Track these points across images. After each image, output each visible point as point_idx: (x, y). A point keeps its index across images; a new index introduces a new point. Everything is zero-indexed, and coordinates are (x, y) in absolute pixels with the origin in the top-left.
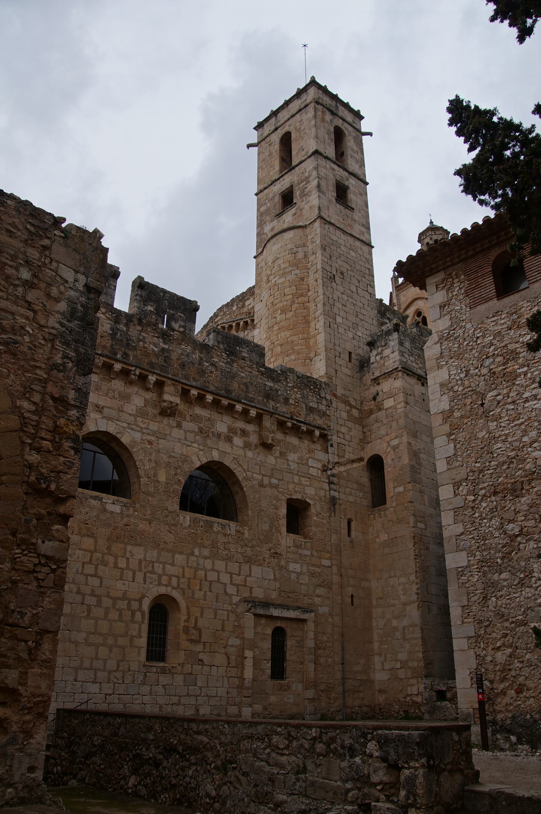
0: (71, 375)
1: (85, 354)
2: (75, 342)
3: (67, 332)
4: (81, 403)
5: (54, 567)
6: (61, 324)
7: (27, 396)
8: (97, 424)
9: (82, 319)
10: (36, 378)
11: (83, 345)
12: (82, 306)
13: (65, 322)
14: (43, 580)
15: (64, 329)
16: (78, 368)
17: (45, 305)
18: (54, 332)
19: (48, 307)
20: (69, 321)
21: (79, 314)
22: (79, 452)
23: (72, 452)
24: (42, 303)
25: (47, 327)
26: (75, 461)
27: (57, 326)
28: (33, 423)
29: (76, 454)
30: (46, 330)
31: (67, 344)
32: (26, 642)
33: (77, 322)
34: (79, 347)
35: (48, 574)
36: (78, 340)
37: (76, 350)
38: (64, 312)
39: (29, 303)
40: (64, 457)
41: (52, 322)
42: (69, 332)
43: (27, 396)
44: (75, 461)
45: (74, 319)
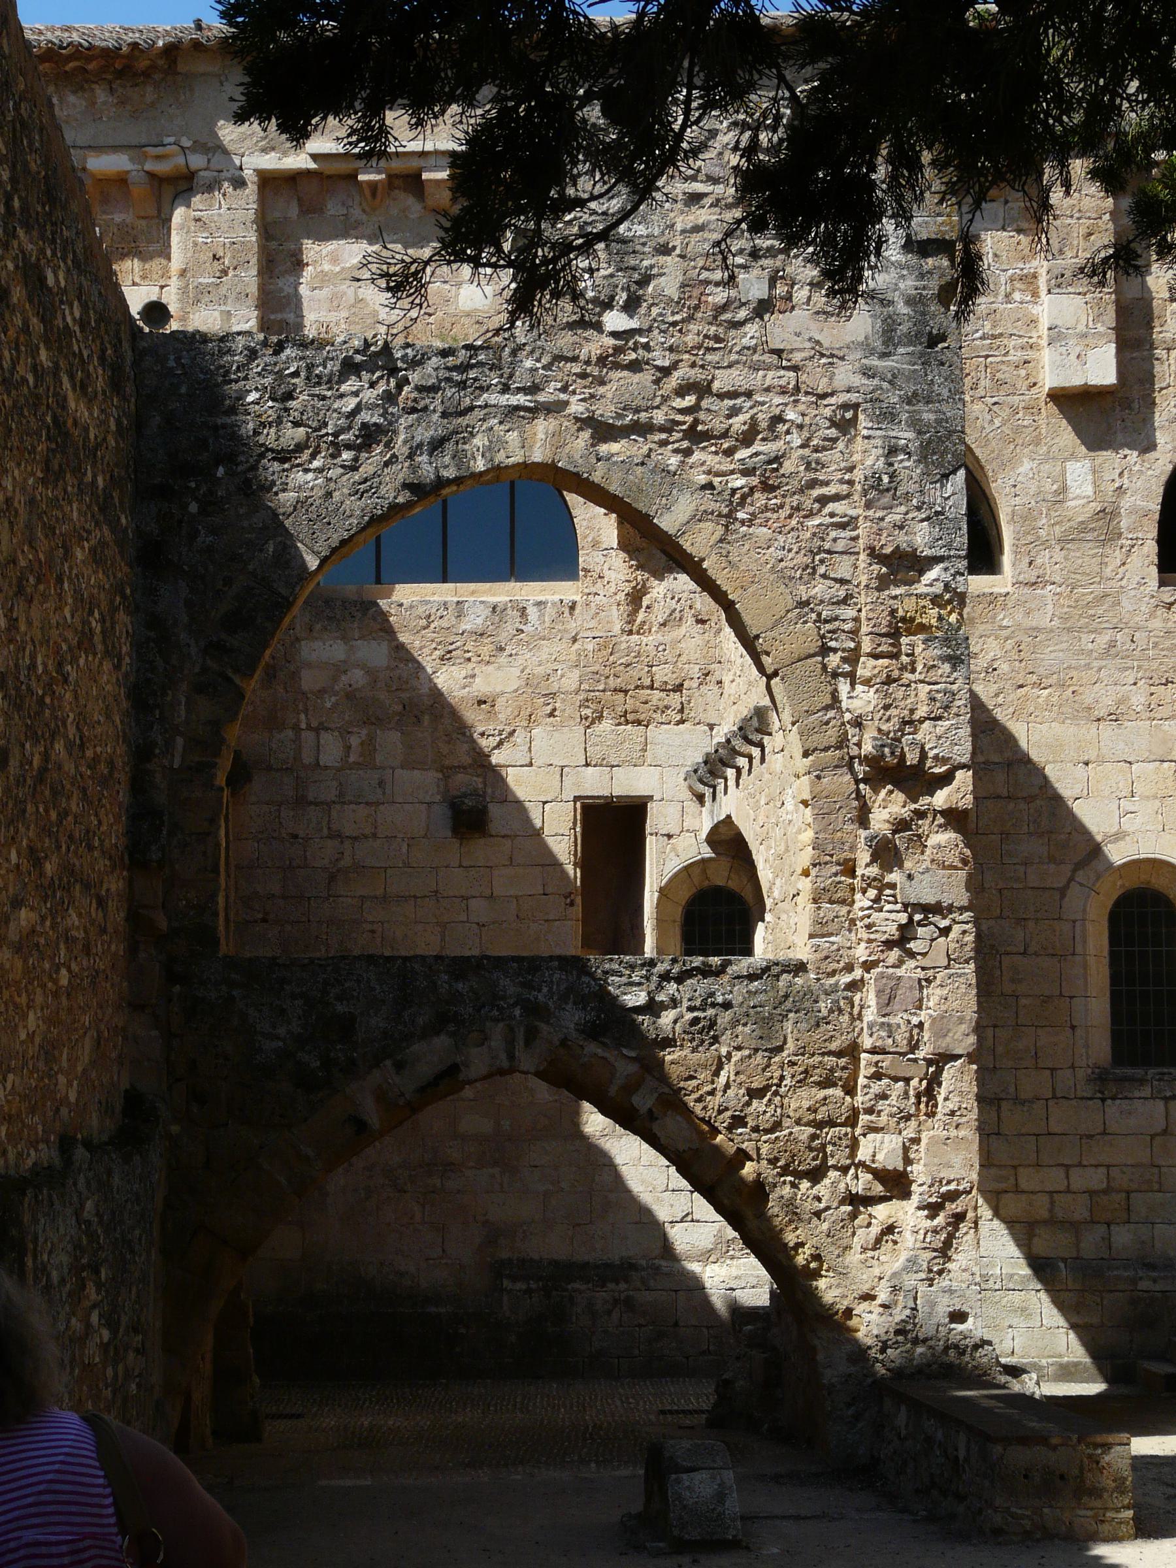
0: (912, 487)
1: (938, 422)
2: (909, 403)
3: (885, 385)
4: (949, 546)
5: (944, 923)
6: (868, 372)
7: (822, 570)
9: (910, 339)
10: (833, 524)
11: (928, 403)
12: (910, 301)
13: (875, 362)
14: (924, 955)
15: (876, 382)
16: (927, 467)
17: (818, 342)
18: (853, 397)
19: (826, 344)
20: (884, 355)
21: (903, 329)
22: (962, 662)
23: (947, 667)
24: (810, 339)
25: (832, 394)
26: (955, 687)
27: (857, 380)
28: (847, 627)
29: (954, 668)
30: (832, 400)
31: (888, 416)
32: (907, 1080)
33: (901, 350)
34: (919, 412)
35: (933, 940)
36: (915, 394)
37: (915, 424)
38: (866, 338)
39: (779, 353)
40: (929, 684)
41: (846, 375)
42: (890, 382)
43: (822, 570)
44: (955, 687)
45: (896, 346)
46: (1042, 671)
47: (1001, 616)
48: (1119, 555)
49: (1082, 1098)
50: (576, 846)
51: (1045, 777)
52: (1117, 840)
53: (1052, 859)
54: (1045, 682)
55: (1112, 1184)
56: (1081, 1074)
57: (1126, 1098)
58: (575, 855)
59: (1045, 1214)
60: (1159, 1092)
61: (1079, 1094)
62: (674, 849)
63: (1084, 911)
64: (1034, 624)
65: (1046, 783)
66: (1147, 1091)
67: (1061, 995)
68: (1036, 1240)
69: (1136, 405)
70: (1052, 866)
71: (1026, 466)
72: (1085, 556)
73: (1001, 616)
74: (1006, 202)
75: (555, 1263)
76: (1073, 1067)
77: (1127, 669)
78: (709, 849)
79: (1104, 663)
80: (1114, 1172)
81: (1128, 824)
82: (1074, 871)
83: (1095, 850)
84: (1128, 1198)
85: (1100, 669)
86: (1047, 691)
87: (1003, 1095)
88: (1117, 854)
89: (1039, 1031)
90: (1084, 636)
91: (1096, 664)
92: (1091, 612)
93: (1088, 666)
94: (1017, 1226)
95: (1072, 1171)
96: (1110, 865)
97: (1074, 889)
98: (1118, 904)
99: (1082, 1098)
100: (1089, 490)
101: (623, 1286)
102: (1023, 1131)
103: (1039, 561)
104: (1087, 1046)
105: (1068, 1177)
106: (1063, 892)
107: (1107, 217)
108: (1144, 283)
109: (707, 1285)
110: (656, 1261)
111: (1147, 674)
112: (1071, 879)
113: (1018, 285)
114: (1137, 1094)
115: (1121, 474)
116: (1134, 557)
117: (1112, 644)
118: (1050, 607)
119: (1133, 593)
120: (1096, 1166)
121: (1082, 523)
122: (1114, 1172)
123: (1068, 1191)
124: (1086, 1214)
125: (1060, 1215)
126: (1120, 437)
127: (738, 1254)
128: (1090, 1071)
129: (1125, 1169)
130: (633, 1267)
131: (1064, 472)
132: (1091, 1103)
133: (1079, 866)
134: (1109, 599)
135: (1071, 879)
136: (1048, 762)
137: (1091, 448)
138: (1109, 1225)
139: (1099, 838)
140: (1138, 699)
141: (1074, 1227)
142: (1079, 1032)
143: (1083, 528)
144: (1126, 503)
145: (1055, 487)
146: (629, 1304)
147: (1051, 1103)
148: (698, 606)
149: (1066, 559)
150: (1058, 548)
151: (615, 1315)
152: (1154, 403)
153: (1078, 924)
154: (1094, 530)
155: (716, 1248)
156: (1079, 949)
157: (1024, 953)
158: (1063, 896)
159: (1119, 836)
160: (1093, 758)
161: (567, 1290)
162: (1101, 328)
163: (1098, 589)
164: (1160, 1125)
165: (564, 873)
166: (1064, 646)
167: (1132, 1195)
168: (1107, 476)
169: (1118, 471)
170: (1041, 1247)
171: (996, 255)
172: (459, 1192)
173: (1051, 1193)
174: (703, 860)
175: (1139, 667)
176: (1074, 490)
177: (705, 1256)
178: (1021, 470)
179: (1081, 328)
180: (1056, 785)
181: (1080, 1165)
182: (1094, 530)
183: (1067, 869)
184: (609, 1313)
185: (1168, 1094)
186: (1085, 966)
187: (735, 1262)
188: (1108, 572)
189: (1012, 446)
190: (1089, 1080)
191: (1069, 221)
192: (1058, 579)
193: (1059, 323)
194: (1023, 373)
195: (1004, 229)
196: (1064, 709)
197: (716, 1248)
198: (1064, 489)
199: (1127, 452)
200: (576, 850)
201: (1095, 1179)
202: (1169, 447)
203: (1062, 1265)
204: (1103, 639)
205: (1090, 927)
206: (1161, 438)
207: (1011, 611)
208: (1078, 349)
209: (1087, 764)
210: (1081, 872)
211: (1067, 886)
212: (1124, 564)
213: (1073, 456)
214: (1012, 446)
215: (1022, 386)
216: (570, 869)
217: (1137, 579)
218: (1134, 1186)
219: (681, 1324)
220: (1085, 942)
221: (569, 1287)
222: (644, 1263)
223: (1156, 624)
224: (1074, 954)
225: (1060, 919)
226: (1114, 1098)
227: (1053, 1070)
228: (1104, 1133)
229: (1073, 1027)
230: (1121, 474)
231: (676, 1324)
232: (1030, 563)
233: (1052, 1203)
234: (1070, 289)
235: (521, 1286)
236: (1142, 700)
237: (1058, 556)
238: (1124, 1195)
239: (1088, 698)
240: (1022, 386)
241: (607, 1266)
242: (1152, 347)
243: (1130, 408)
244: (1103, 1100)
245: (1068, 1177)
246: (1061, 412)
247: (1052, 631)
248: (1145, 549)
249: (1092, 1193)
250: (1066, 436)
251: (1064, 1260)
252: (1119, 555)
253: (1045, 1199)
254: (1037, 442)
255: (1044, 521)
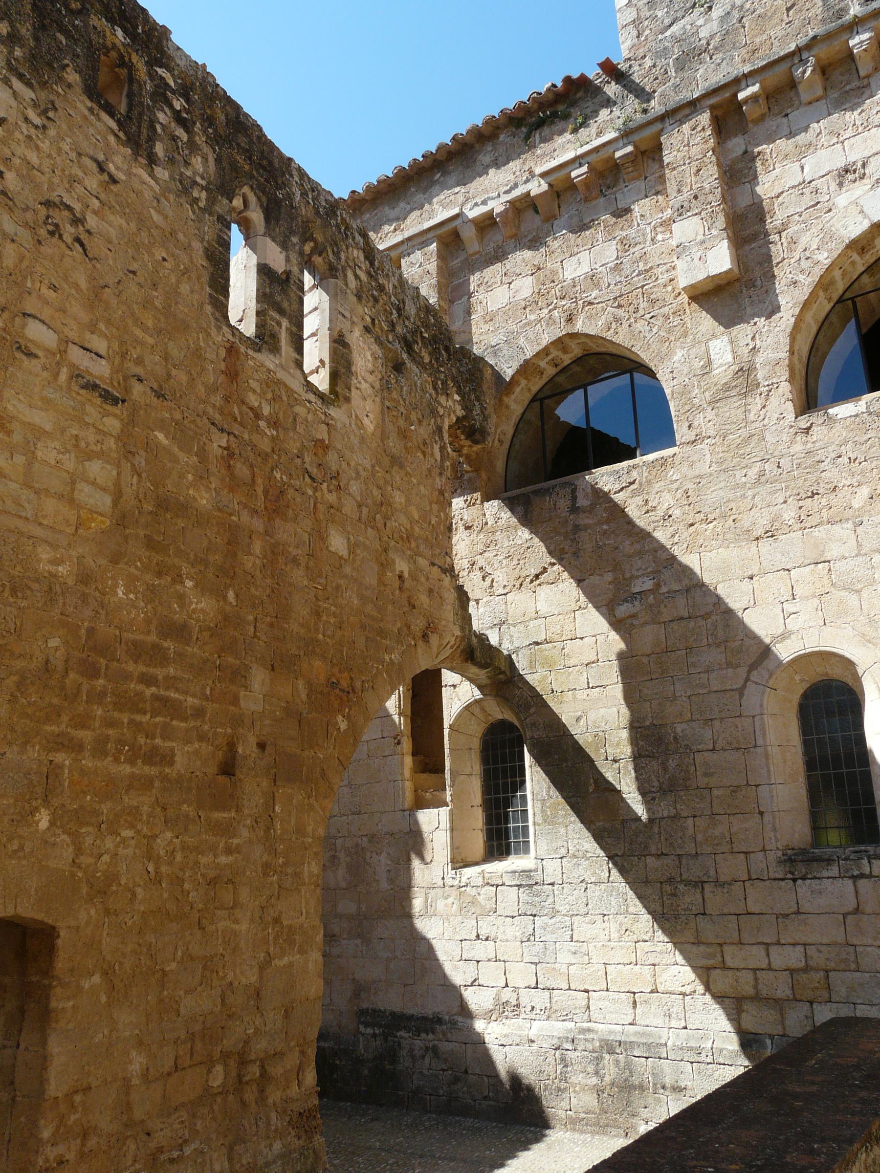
8: (862, 212)
46: (706, 509)
47: (671, 473)
48: (759, 401)
49: (775, 879)
50: (400, 701)
51: (718, 596)
52: (784, 639)
53: (729, 665)
54: (711, 517)
55: (811, 963)
56: (772, 856)
57: (815, 878)
58: (400, 707)
59: (751, 991)
60: (847, 871)
61: (772, 875)
62: (457, 695)
63: (761, 706)
64: (697, 473)
65: (719, 601)
66: (834, 871)
67: (748, 784)
68: (744, 1015)
69: (759, 283)
70: (730, 670)
71: (679, 355)
72: (732, 409)
73: (671, 473)
74: (646, 178)
75: (393, 1014)
76: (764, 850)
77: (776, 491)
78: (478, 692)
79: (757, 490)
80: (812, 950)
81: (793, 624)
82: (749, 672)
83: (766, 651)
84: (828, 977)
85: (754, 497)
86: (711, 525)
87: (705, 879)
88: (785, 652)
89: (731, 818)
90: (737, 473)
91: (750, 493)
92: (741, 452)
93: (743, 496)
94: (727, 1001)
95: (773, 950)
96: (780, 663)
97: (751, 687)
98: (805, 696)
99: (775, 879)
100: (729, 358)
101: (431, 1036)
102: (726, 911)
103: (696, 423)
104: (774, 830)
105: (768, 955)
106: (741, 691)
107: (711, 153)
108: (753, 192)
109: (487, 1041)
110: (455, 1017)
111: (795, 492)
112: (747, 679)
113: (659, 229)
114: (825, 874)
115: (753, 338)
116: (772, 399)
117: (762, 473)
118: (708, 456)
119: (774, 428)
120: (794, 945)
121: (726, 384)
122: (812, 950)
123: (770, 969)
124: (789, 992)
125: (764, 992)
126: (749, 310)
127: (511, 1015)
128: (780, 853)
129: (823, 948)
130: (439, 1021)
131: (708, 351)
132: (782, 883)
133: (753, 667)
134: (756, 437)
135: (747, 679)
136: (718, 583)
137: (727, 327)
138: (811, 1003)
139: (767, 640)
140: (789, 514)
141: (778, 1004)
142: (767, 817)
143: (727, 387)
144: (759, 359)
145: (702, 363)
146: (435, 1050)
147: (747, 883)
148: (465, 518)
149: (717, 415)
150: (710, 408)
151: (427, 1060)
152: (774, 276)
153: (756, 718)
154: (736, 386)
155: (495, 1009)
156: (760, 742)
157: (713, 750)
158: (741, 695)
159: (785, 636)
160: (755, 573)
161: (396, 1037)
162: (714, 232)
163: (744, 433)
164: (852, 904)
165: (393, 720)
166: (722, 484)
167: (830, 974)
168: (742, 343)
169: (750, 337)
170: (748, 1023)
171: (642, 216)
172: (339, 956)
173: (755, 970)
174: (476, 701)
175: (787, 487)
176: (717, 360)
177: (488, 1015)
178: (676, 358)
179: (700, 237)
180: (727, 601)
181: (778, 943)
182: (736, 386)
183: (742, 671)
184: (423, 1057)
185: (856, 873)
186: (767, 756)
187: (508, 1022)
188: (752, 417)
189: (667, 344)
190: (780, 862)
191: (683, 167)
192: (712, 433)
193: (683, 240)
194: (669, 288)
195: (646, 197)
196: (727, 536)
197: (495, 1009)
198: (710, 362)
199: (756, 319)
200: (400, 704)
201: (794, 957)
202: (790, 305)
203: (768, 1042)
204: (753, 473)
205: (769, 721)
206: (782, 300)
207: (678, 467)
208: (699, 254)
209: (751, 578)
210: (755, 673)
211: (744, 686)
212: (764, 407)
213: (714, 336)
214: (667, 344)
215: (670, 298)
216: (396, 718)
217: (777, 416)
218: (832, 965)
219: (470, 1072)
220: (764, 734)
221: (398, 1034)
222: (447, 1018)
223: (798, 448)
224: (755, 746)
225: (741, 716)
226: (804, 878)
227: (746, 853)
228: (798, 912)
229: (761, 813)
230: (753, 338)
231: (466, 1072)
232: (690, 427)
233: (756, 979)
234: (689, 214)
235: (369, 1031)
236: (793, 514)
237: (710, 414)
238: (822, 974)
239: (746, 522)
240: (670, 298)
241: (425, 1019)
242: (767, 234)
243: (754, 286)
244: (794, 880)
245: (768, 955)
246: (700, 306)
247: (711, 475)
248: (780, 390)
249: (792, 971)
250: (706, 322)
251: (771, 1037)
252: (759, 401)
253: (750, 976)
254: (685, 334)
255: (696, 391)
